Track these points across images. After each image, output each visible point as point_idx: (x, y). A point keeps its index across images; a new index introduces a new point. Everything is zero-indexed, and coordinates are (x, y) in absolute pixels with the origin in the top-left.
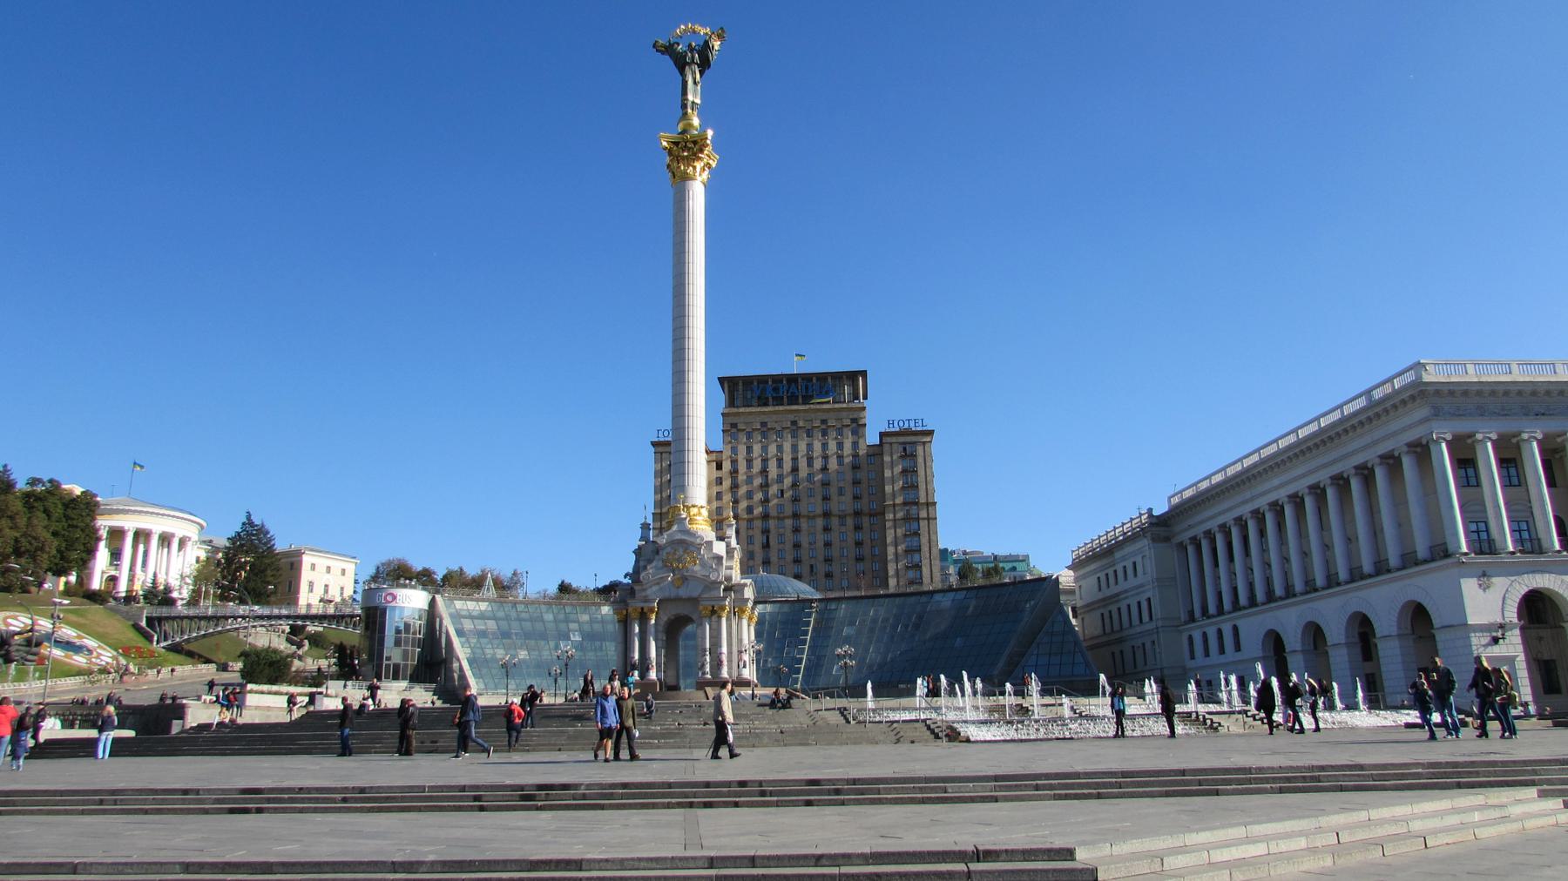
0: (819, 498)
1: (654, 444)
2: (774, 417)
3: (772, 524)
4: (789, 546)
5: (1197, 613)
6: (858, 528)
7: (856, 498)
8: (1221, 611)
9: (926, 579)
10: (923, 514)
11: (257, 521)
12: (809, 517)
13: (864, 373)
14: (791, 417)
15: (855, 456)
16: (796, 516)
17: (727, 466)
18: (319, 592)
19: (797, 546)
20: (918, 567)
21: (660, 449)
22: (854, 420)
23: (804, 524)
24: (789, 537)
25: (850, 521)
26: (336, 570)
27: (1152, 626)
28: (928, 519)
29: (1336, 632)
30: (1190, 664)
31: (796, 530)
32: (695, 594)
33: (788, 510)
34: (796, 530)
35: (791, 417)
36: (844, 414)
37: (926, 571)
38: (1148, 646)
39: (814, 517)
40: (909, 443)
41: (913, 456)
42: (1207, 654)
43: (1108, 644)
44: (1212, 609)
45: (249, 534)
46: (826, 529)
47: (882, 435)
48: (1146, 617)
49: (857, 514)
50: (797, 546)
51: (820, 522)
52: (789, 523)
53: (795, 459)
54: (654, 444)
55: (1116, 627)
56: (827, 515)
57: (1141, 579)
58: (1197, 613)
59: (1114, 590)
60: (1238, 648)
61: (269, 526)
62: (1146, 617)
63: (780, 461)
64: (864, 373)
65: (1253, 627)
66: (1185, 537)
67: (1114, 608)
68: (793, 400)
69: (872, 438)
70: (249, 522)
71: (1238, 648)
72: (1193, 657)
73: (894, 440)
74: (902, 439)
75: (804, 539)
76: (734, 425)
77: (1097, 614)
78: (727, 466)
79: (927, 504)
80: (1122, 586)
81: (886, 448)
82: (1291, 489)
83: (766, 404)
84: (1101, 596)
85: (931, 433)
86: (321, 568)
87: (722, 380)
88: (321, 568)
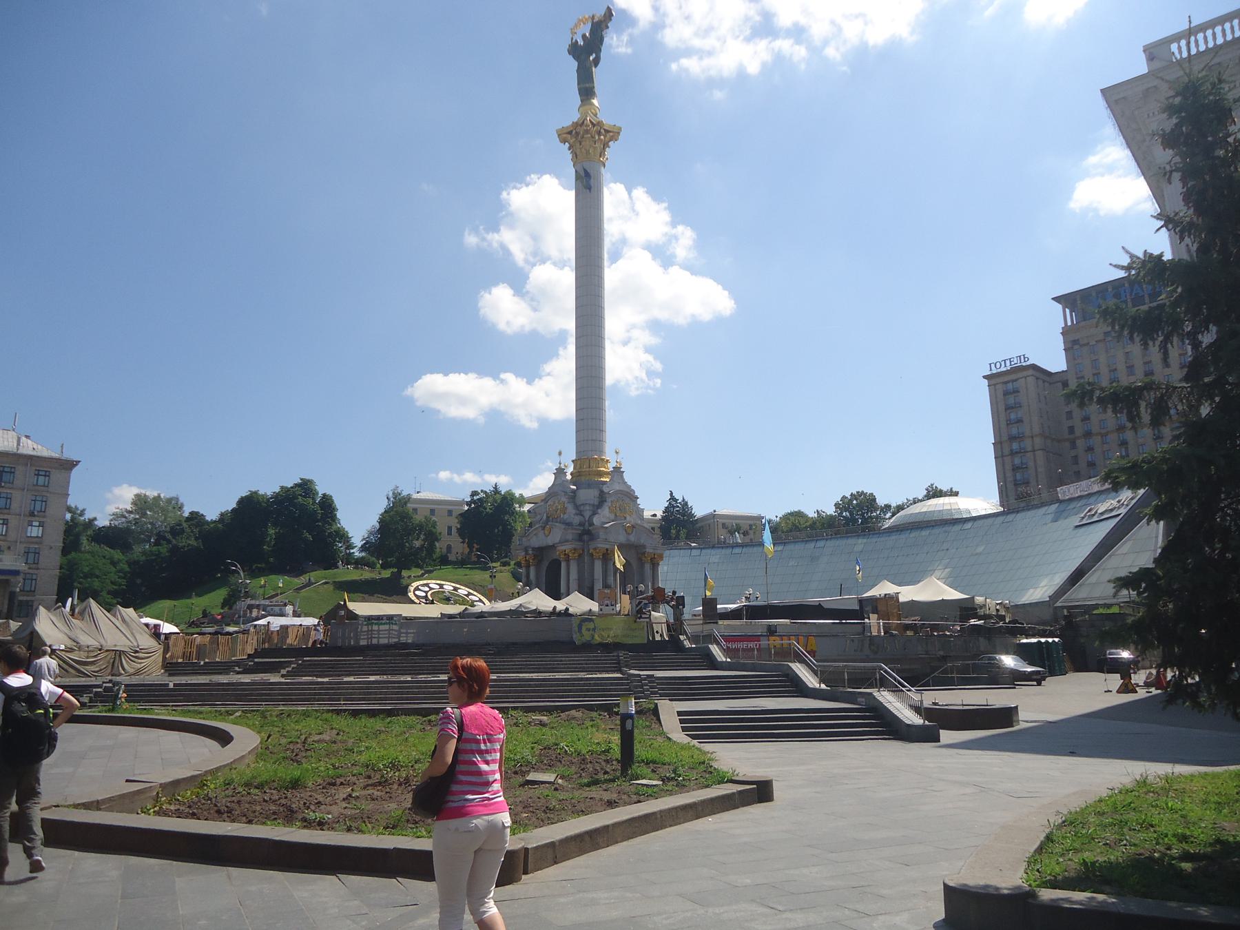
11: (679, 497)
21: (993, 382)
70: (672, 498)
76: (1075, 342)
87: (1056, 299)
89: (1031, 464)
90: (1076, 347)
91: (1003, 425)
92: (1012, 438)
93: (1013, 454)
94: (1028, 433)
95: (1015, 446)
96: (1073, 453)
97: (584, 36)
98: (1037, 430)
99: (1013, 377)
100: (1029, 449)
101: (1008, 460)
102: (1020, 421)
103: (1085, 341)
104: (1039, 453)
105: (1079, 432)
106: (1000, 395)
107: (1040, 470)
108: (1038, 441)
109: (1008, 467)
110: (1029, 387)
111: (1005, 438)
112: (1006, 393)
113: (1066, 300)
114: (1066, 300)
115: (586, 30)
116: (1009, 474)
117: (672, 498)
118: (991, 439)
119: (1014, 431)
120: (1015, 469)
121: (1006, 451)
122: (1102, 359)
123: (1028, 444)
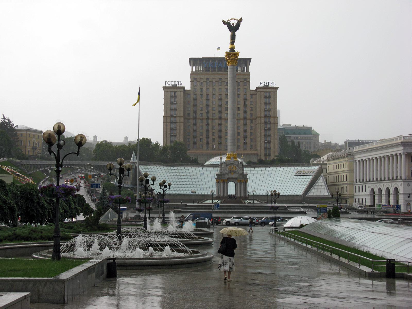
1: (164, 88)
2: (213, 76)
3: (210, 121)
4: (217, 131)
5: (358, 181)
6: (245, 125)
7: (245, 112)
8: (363, 182)
9: (272, 148)
10: (272, 121)
13: (250, 60)
14: (219, 77)
15: (245, 95)
17: (192, 96)
20: (269, 142)
21: (167, 90)
22: (245, 79)
25: (242, 122)
27: (346, 182)
28: (274, 123)
29: (384, 191)
30: (355, 194)
32: (236, 177)
35: (219, 77)
36: (241, 76)
37: (272, 145)
38: (345, 188)
40: (268, 93)
41: (269, 97)
42: (359, 192)
43: (335, 185)
44: (361, 181)
47: (257, 88)
48: (345, 180)
49: (245, 119)
52: (217, 121)
53: (220, 95)
54: (164, 88)
55: (337, 181)
57: (345, 169)
58: (358, 181)
59: (337, 170)
60: (366, 191)
62: (345, 180)
63: (214, 94)
64: (250, 60)
65: (369, 187)
66: (357, 159)
67: (337, 175)
68: (220, 69)
69: (253, 87)
71: (366, 191)
72: (356, 192)
73: (262, 90)
74: (265, 90)
77: (333, 176)
78: (192, 96)
79: (274, 117)
80: (340, 170)
81: (259, 93)
82: (379, 155)
83: (209, 71)
84: (334, 171)
85: (277, 88)
87: (190, 59)
89: (178, 128)
90: (195, 81)
91: (169, 110)
92: (172, 116)
93: (171, 123)
94: (178, 115)
95: (172, 119)
97: (233, 24)
98: (182, 115)
99: (175, 90)
100: (178, 121)
101: (169, 124)
102: (175, 110)
103: (199, 80)
105: (192, 116)
106: (169, 97)
108: (182, 119)
109: (169, 127)
110: (180, 95)
111: (169, 115)
112: (171, 97)
113: (194, 62)
114: (194, 62)
115: (236, 22)
117: (4, 118)
119: (173, 113)
120: (172, 129)
121: (169, 121)
122: (204, 89)
123: (178, 119)
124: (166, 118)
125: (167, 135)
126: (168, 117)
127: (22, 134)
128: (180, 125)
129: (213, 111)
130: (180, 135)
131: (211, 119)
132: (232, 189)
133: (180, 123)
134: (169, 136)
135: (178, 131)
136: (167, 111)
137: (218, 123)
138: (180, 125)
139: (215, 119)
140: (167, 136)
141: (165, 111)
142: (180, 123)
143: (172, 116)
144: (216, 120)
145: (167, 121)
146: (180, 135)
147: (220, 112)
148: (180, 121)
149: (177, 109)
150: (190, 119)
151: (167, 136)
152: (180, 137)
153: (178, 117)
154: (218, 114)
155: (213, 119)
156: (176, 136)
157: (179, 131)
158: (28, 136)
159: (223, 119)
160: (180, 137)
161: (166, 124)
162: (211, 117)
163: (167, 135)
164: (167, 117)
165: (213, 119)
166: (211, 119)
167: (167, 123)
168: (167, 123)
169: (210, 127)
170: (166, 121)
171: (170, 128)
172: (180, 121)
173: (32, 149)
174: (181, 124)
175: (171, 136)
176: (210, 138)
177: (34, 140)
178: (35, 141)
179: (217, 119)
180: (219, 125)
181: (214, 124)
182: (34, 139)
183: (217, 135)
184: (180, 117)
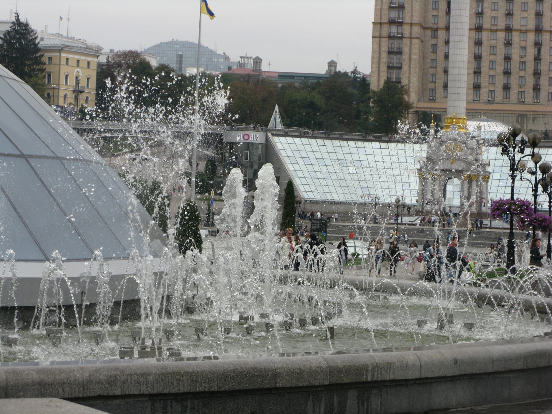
0: (532, 14)
3: (485, 35)
4: (500, 58)
12: (521, 31)
16: (508, 29)
18: (72, 82)
19: (508, 59)
23: (516, 37)
24: (501, 50)
26: (83, 64)
31: (508, 44)
33: (502, 24)
34: (508, 44)
39: (526, 31)
45: (17, 32)
46: (538, 45)
50: (508, 59)
51: (531, 37)
56: (538, 30)
61: (33, 26)
75: (515, 53)
86: (73, 63)
88: (73, 63)
89: (406, 50)
92: (392, 22)
93: (390, 37)
94: (407, 20)
95: (394, 30)
96: (433, 41)
100: (407, 34)
101: (385, 41)
104: (416, 42)
107: (414, 57)
108: (416, 30)
111: (385, 20)
116: (384, 56)
118: (370, 17)
119: (394, 15)
121: (385, 33)
123: (406, 30)
124: (378, 26)
125: (379, 65)
126: (384, 23)
127: (50, 59)
128: (411, 43)
129: (493, 12)
130: (410, 67)
131: (487, 30)
132: (454, 194)
133: (411, 38)
134: (384, 68)
135: (405, 57)
136: (381, 11)
137: (503, 40)
138: (411, 43)
139: (497, 30)
140: (379, 69)
141: (379, 11)
142: (411, 38)
143: (392, 22)
144: (499, 33)
145: (380, 33)
146: (410, 67)
147: (509, 14)
148: (411, 34)
149: (406, 6)
150: (437, 29)
151: (379, 69)
152: (410, 70)
153: (407, 24)
154: (504, 19)
155: (491, 30)
156: (400, 68)
157: (408, 56)
158: (63, 62)
159: (517, 30)
160: (410, 70)
161: (377, 39)
162: (487, 24)
163: (379, 65)
164: (381, 24)
165: (491, 30)
166: (487, 30)
167: (380, 37)
168: (380, 37)
169: (485, 51)
170: (377, 34)
171: (387, 50)
172: (411, 34)
173: (74, 91)
174: (413, 40)
175: (389, 67)
176: (482, 75)
177: (78, 72)
178: (81, 74)
179: (501, 30)
180: (505, 44)
181: (493, 43)
182: (78, 69)
183: (500, 68)
184: (411, 24)
